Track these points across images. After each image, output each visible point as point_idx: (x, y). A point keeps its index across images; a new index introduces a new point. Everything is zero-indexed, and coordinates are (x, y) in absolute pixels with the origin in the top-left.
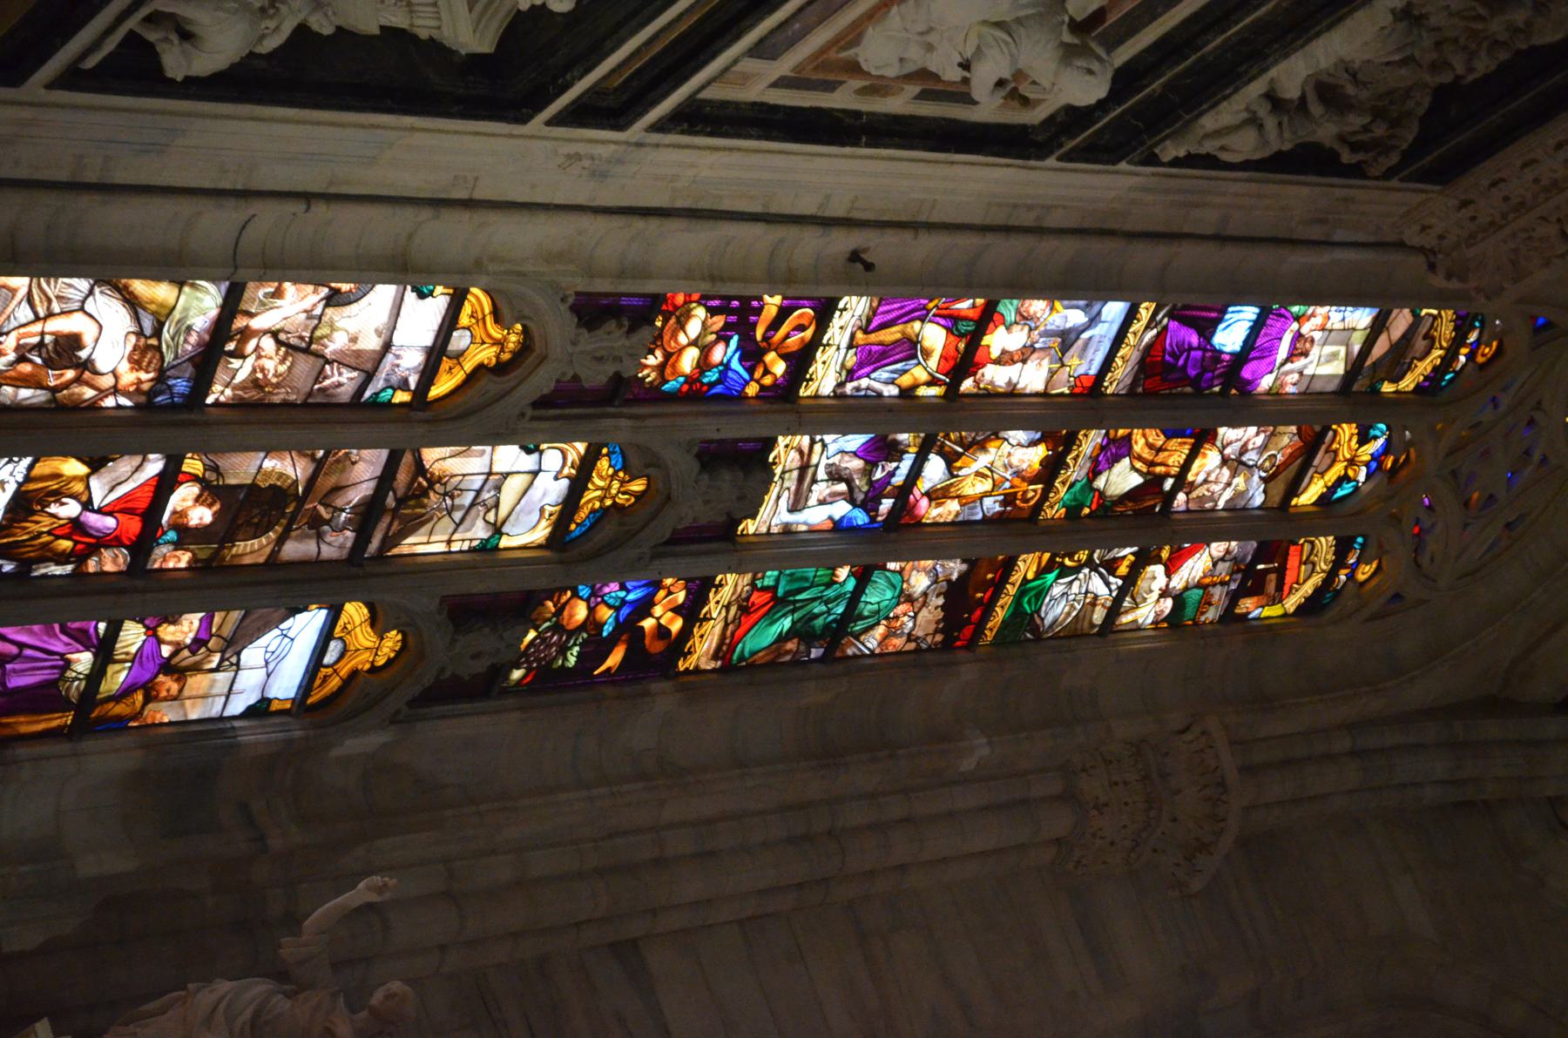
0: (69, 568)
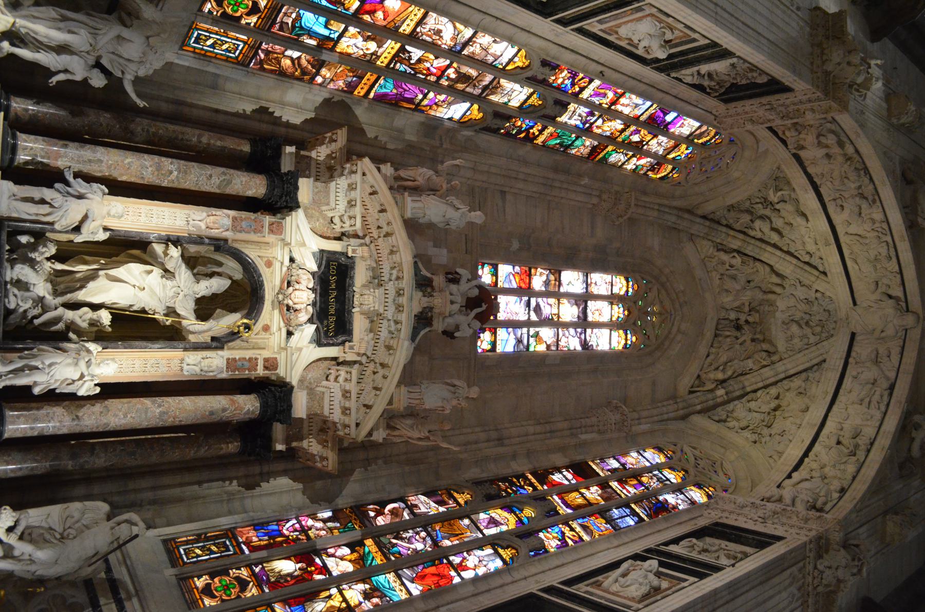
0: (424, 77)
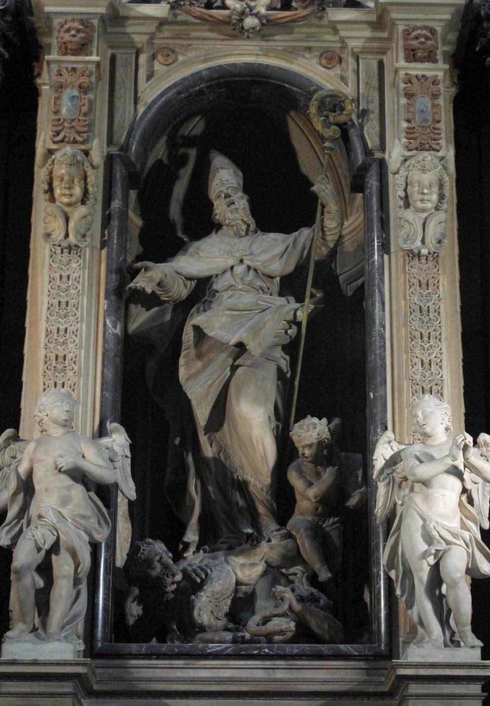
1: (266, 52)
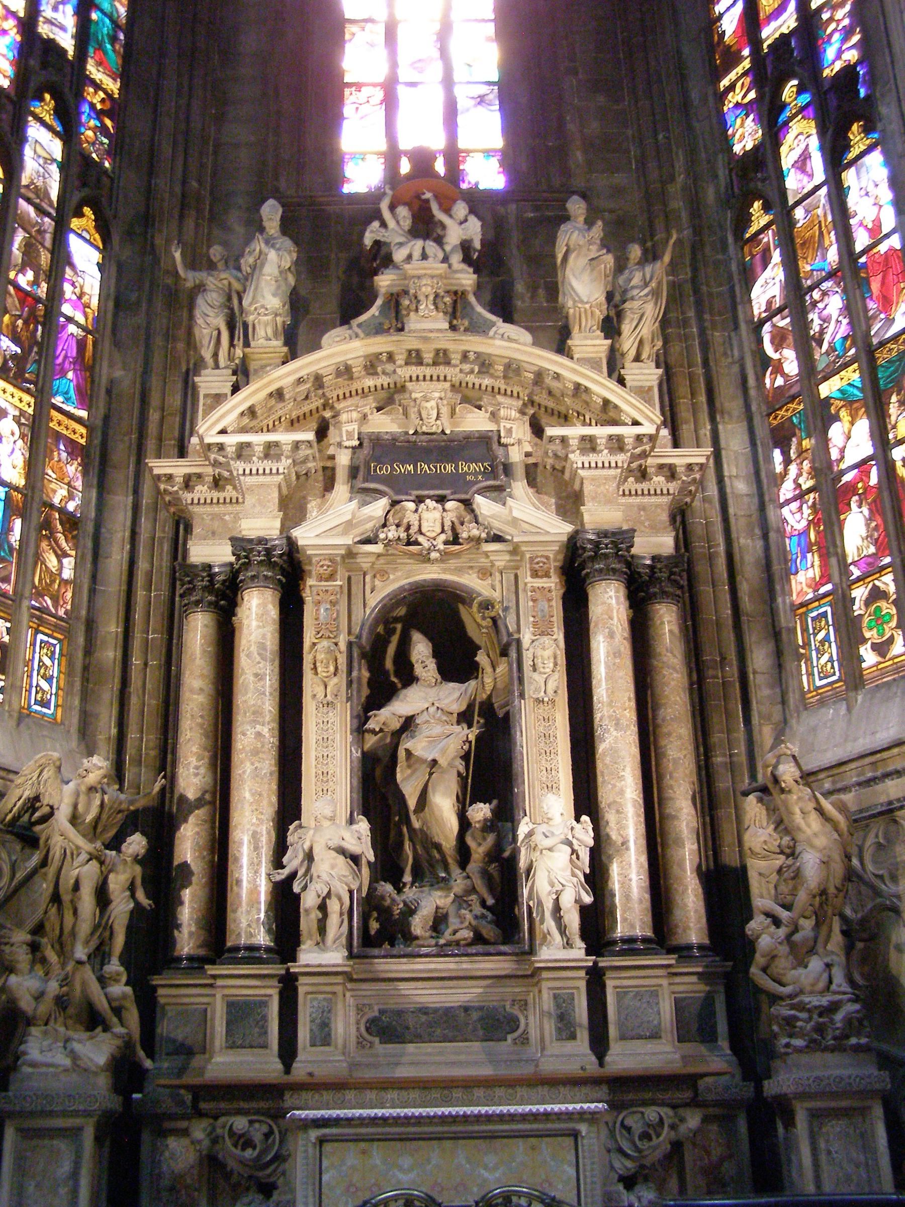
0: (40, 328)
1: (445, 571)
